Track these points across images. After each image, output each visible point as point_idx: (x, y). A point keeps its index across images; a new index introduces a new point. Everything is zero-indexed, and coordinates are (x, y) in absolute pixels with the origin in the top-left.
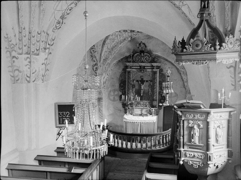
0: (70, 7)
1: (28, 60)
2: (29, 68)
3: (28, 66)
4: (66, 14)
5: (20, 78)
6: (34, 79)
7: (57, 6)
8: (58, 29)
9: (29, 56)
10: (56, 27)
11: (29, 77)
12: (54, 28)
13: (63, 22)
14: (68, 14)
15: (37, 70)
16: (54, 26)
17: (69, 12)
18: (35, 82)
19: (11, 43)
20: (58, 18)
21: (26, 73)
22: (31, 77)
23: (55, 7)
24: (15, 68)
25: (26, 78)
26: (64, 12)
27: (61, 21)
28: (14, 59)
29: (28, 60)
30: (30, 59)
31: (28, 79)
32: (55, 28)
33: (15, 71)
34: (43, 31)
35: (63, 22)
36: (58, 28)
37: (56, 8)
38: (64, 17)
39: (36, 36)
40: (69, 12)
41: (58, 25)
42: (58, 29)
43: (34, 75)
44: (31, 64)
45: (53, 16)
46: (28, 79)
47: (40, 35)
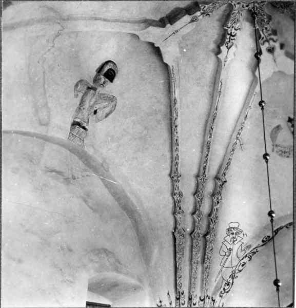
0: (242, 261)
4: (237, 271)
7: (226, 261)
8: (227, 292)
10: (224, 290)
12: (222, 291)
13: (233, 282)
14: (240, 271)
16: (222, 289)
17: (241, 268)
20: (227, 278)
23: (222, 265)
26: (234, 268)
27: (231, 282)
32: (223, 292)
34: (207, 296)
35: (233, 282)
36: (227, 291)
38: (234, 276)
39: (197, 303)
40: (241, 268)
41: (227, 287)
42: (227, 292)
45: (220, 275)
47: (203, 302)
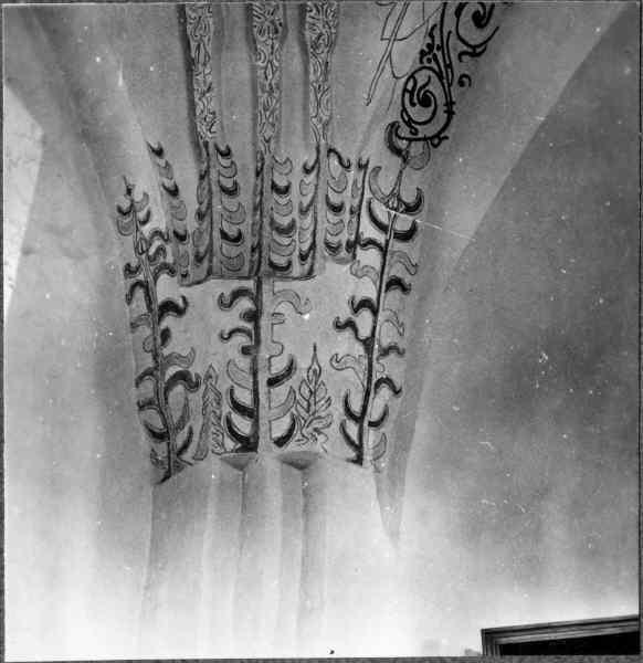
1: (245, 304)
2: (245, 351)
3: (241, 340)
5: (197, 430)
6: (286, 422)
9: (250, 284)
11: (250, 413)
15: (303, 363)
18: (292, 447)
19: (147, 230)
21: (224, 386)
22: (263, 412)
23: (387, 34)
24: (171, 371)
25: (229, 421)
28: (169, 321)
29: (245, 304)
30: (257, 299)
31: (243, 426)
33: (168, 389)
37: (395, 33)
39: (295, 189)
40: (475, 36)
43: (281, 392)
44: (257, 328)
46: (243, 426)
